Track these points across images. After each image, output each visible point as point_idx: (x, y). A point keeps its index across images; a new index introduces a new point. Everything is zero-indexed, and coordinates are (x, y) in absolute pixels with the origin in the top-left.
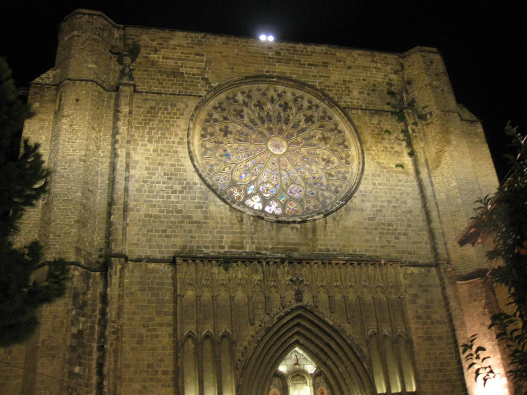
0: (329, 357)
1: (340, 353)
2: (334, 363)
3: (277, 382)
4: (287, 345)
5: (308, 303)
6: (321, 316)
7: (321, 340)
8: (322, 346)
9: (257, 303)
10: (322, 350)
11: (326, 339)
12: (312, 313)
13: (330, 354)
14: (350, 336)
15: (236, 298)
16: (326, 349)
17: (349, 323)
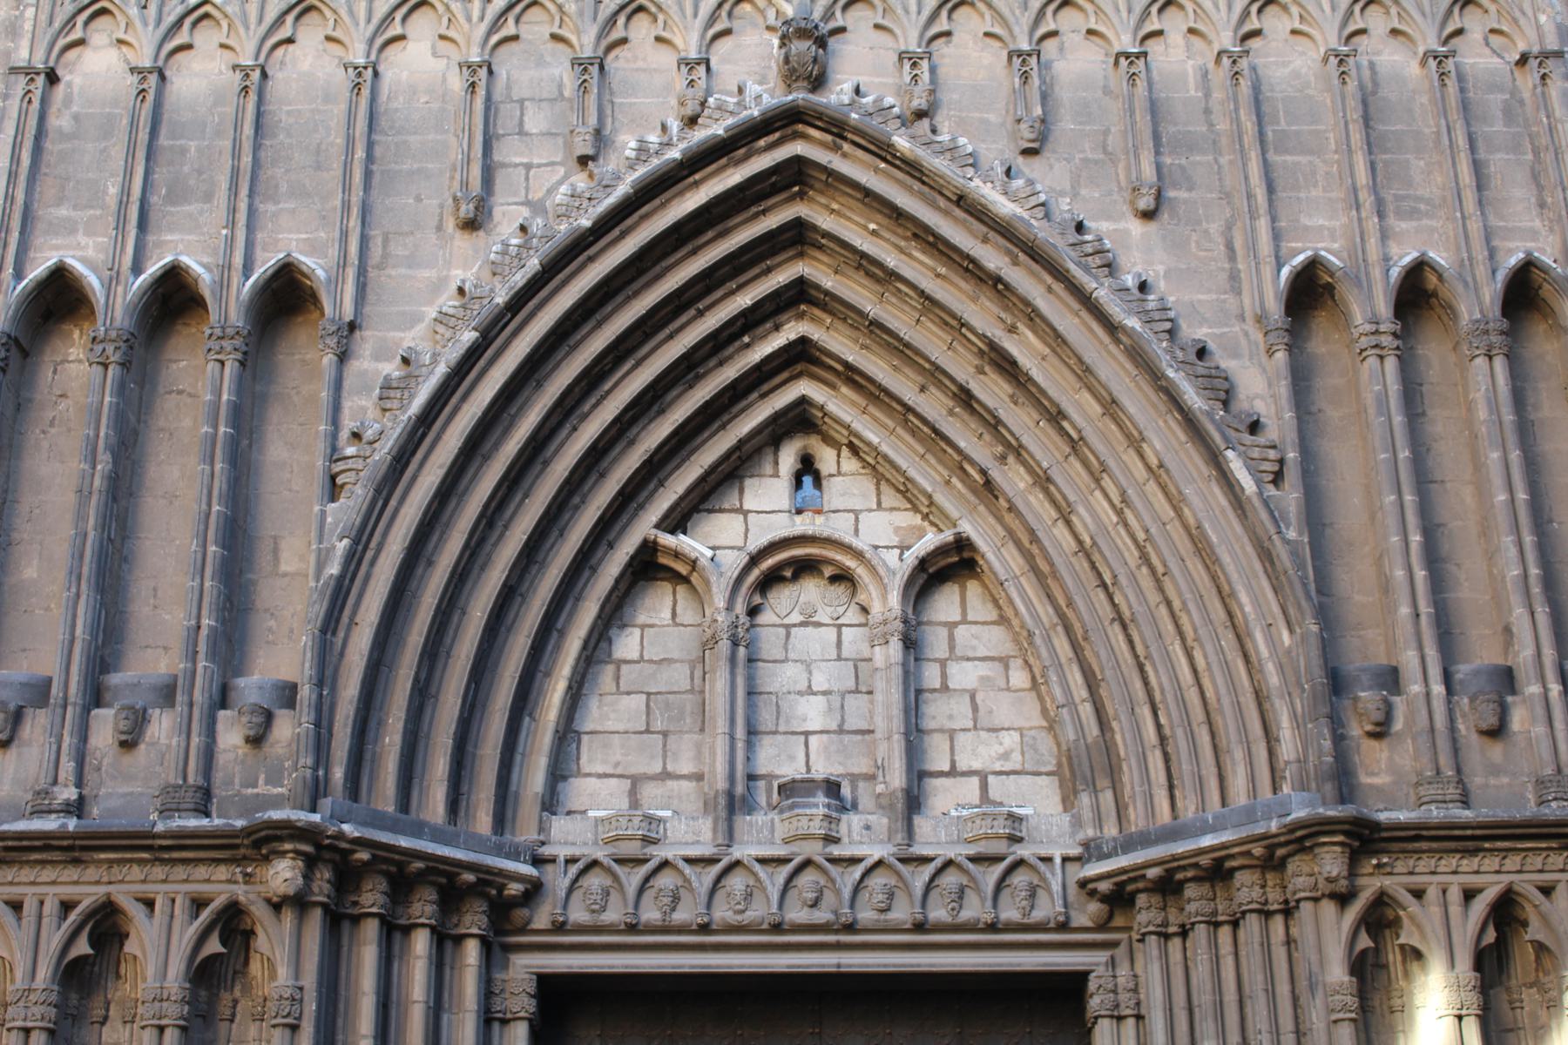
0: (1014, 450)
1: (1081, 408)
2: (1043, 481)
3: (666, 614)
4: (729, 373)
5: (857, 91)
6: (938, 164)
7: (957, 326)
8: (961, 367)
9: (521, 102)
10: (965, 398)
11: (982, 315)
12: (882, 150)
13: (1020, 420)
14: (1143, 287)
15: (389, 74)
16: (992, 391)
17: (1148, 215)
